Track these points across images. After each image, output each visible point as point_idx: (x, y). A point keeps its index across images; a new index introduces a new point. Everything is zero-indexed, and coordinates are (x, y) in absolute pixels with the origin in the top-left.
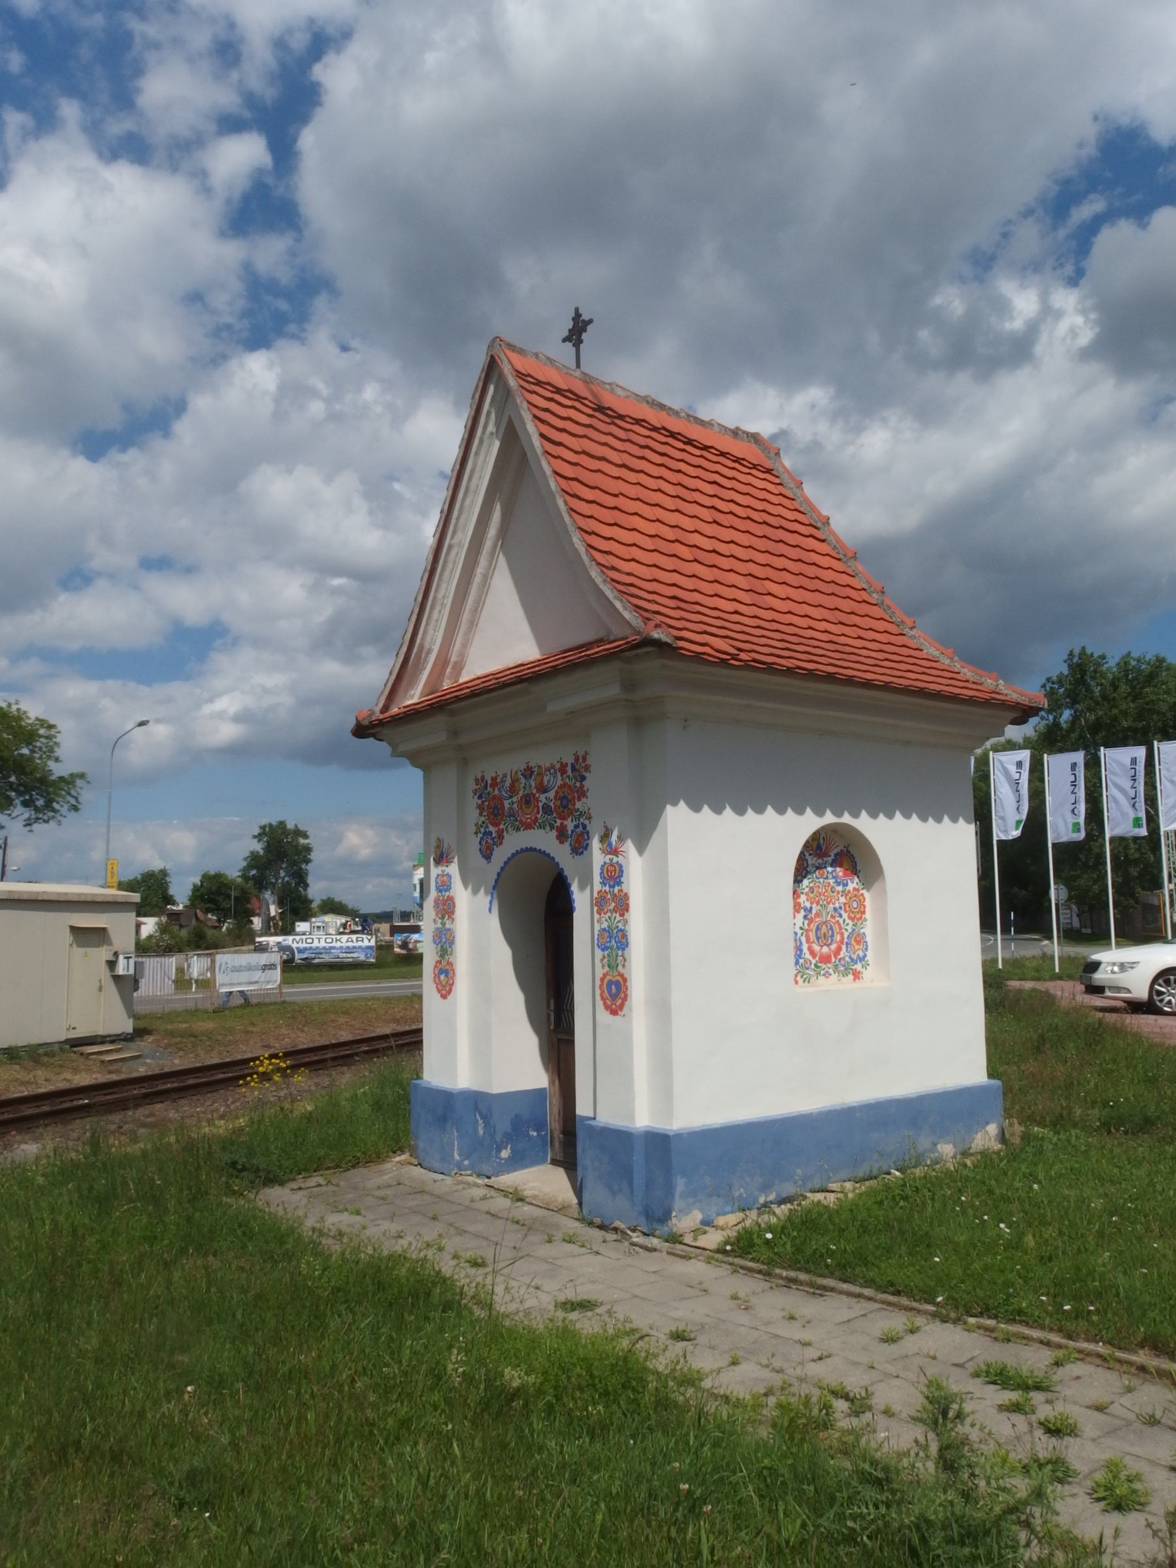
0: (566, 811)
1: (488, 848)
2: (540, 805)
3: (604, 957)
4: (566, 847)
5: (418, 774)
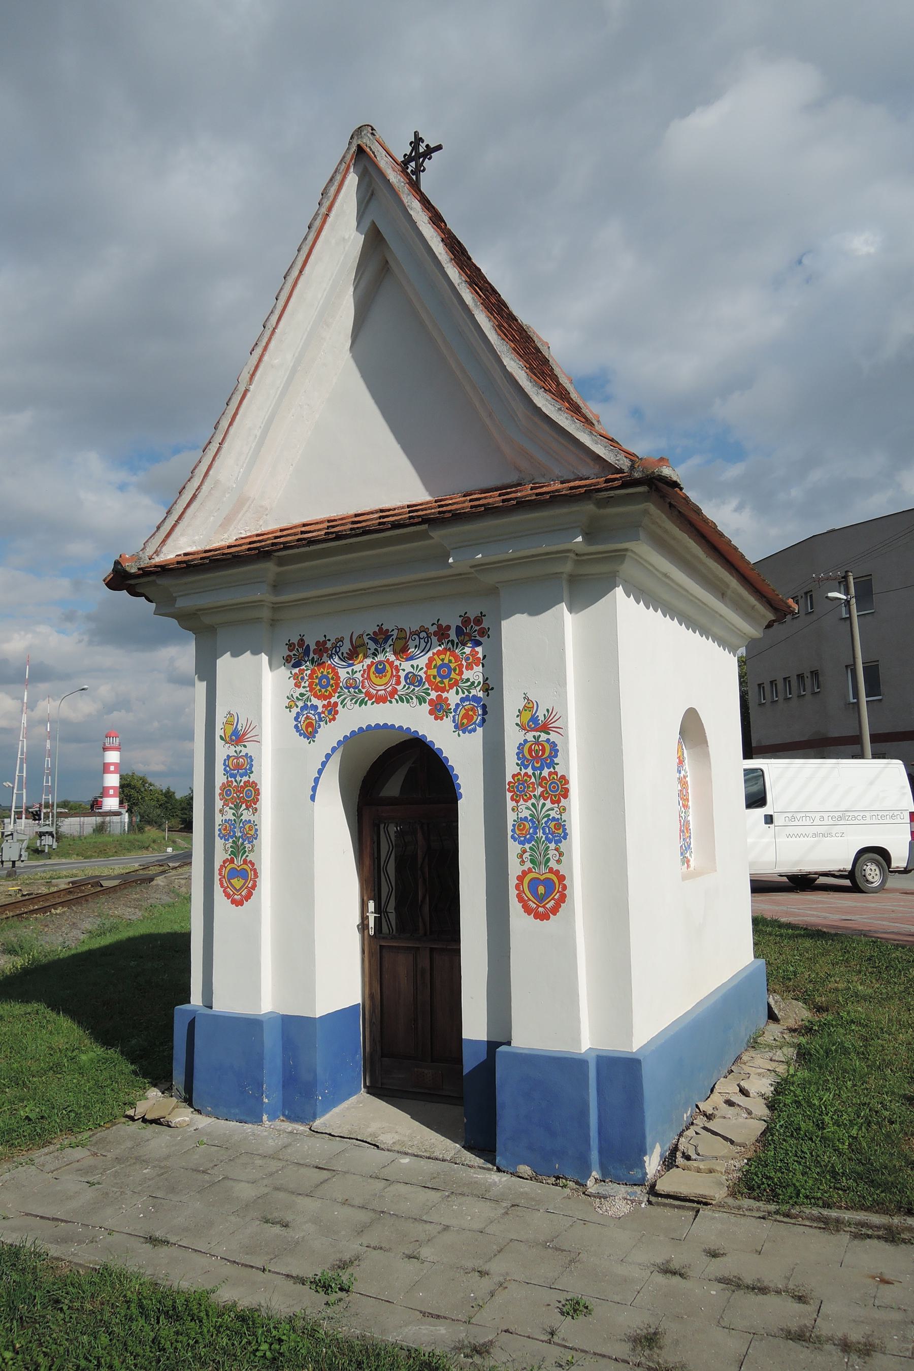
0: (446, 681)
1: (310, 725)
2: (402, 674)
3: (524, 851)
4: (448, 723)
5: (195, 636)
